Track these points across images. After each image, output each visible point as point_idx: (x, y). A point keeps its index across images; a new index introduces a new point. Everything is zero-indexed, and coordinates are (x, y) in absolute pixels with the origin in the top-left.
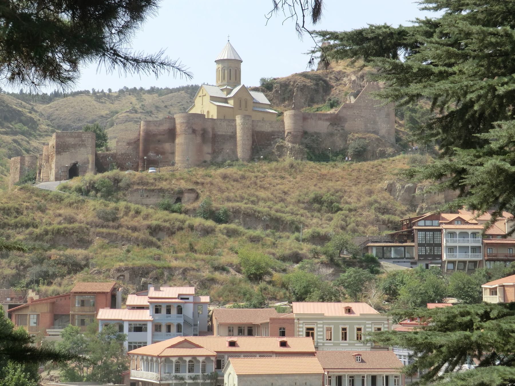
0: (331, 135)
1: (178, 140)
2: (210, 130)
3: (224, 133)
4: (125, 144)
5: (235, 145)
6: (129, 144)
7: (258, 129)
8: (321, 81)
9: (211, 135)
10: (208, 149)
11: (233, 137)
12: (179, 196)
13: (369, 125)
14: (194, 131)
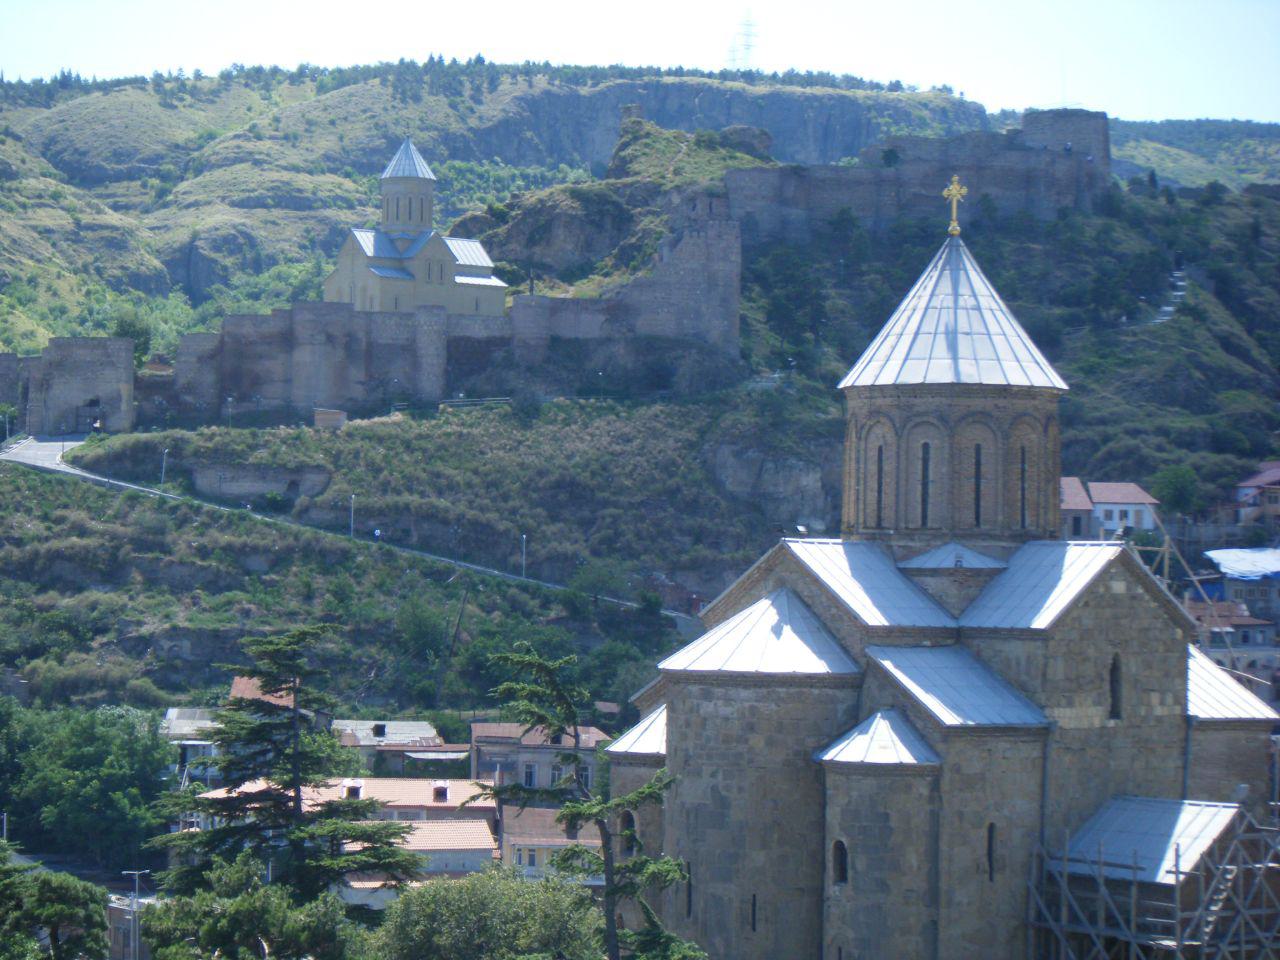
0: (609, 340)
1: (303, 355)
2: (361, 335)
3: (390, 341)
4: (194, 359)
5: (416, 365)
6: (200, 359)
7: (458, 332)
8: (608, 207)
9: (364, 345)
10: (357, 373)
11: (410, 349)
12: (294, 477)
13: (685, 321)
14: (330, 339)
